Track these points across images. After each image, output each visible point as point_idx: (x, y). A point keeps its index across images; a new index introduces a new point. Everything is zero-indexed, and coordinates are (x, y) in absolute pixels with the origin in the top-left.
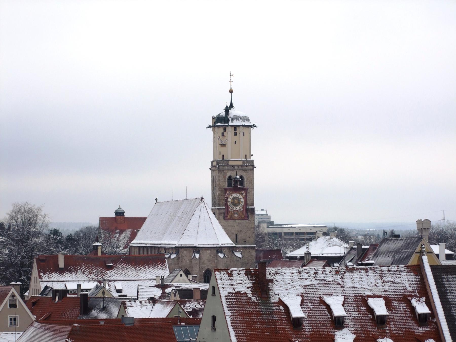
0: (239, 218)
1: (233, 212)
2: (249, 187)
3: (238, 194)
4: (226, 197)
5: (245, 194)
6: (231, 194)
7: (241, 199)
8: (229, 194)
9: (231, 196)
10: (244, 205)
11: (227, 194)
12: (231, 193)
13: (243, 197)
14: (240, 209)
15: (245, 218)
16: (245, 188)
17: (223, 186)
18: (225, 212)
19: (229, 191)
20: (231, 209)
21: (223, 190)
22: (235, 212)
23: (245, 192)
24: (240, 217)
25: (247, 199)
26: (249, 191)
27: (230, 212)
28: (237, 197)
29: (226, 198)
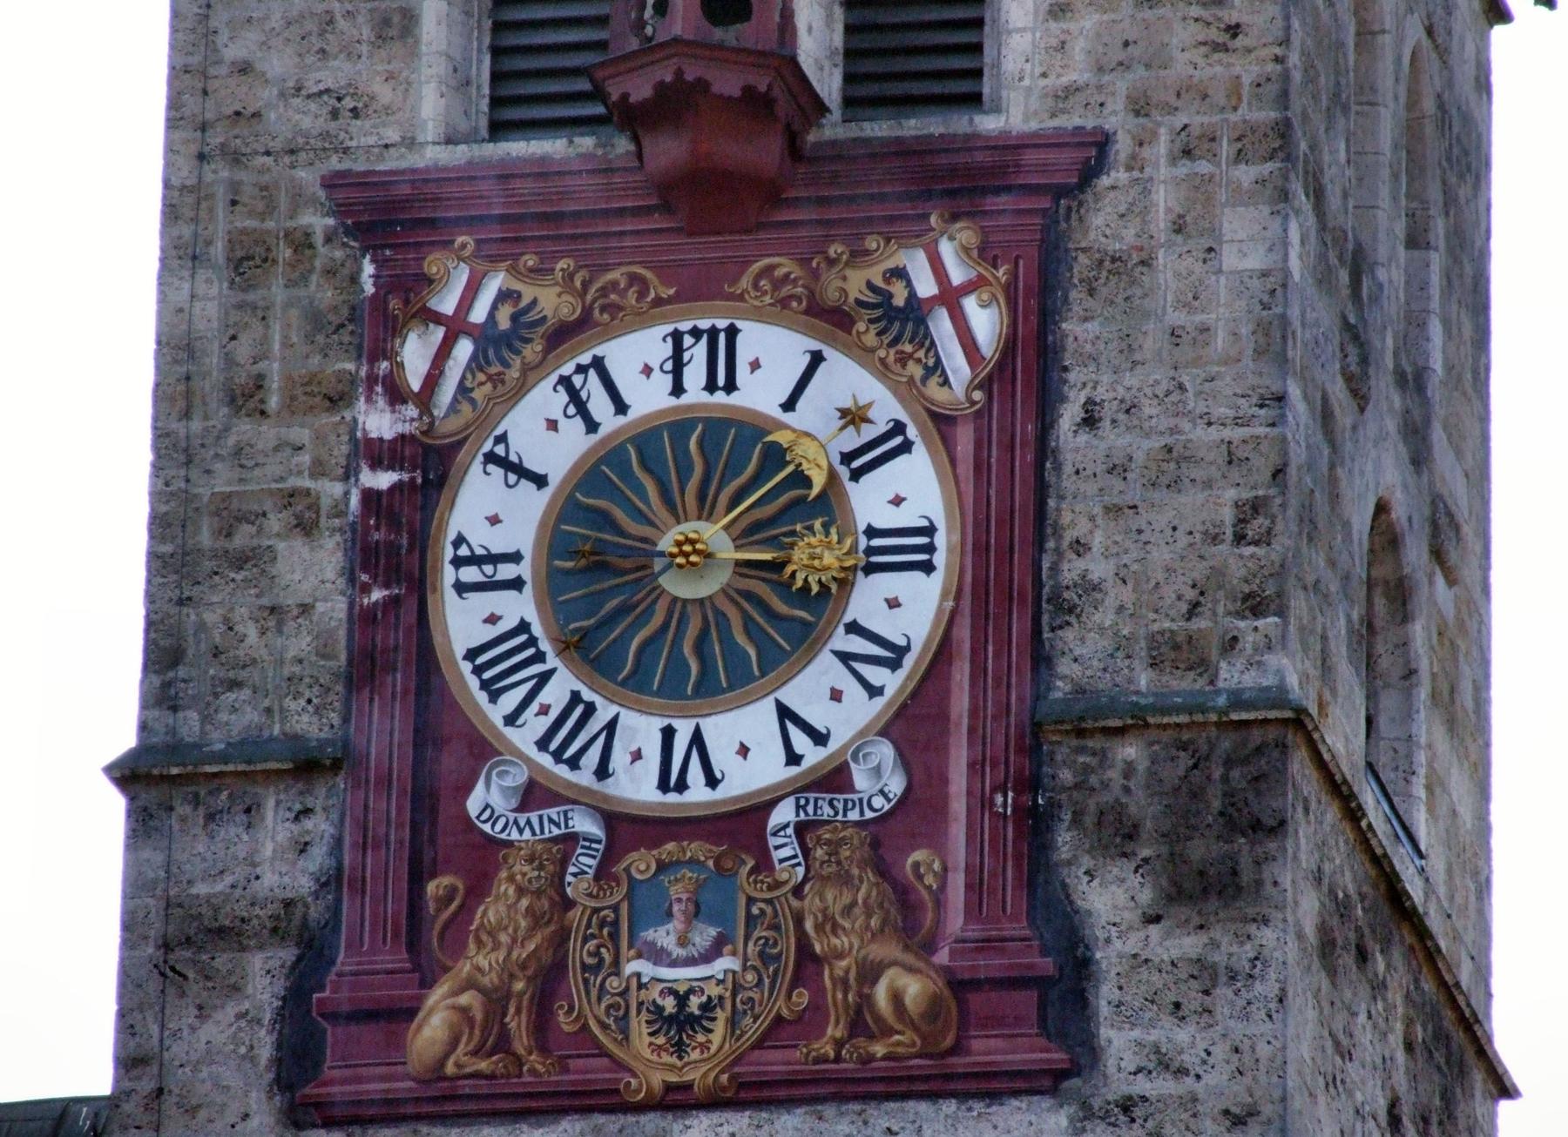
0: (776, 1062)
1: (589, 863)
2: (1116, 119)
3: (756, 339)
4: (380, 422)
5: (985, 321)
6: (563, 335)
7: (861, 461)
8: (492, 343)
9: (546, 398)
10: (942, 653)
11: (415, 354)
12: (552, 302)
13: (941, 422)
14: (835, 779)
15: (987, 1049)
16: (1011, 147)
17: (309, 119)
18: (330, 882)
19: (488, 257)
20: (534, 795)
21: (318, 222)
22: (640, 863)
23: (986, 253)
24: (809, 1021)
25: (1044, 448)
26: (1139, 210)
27: (478, 888)
28: (751, 429)
29: (378, 454)
